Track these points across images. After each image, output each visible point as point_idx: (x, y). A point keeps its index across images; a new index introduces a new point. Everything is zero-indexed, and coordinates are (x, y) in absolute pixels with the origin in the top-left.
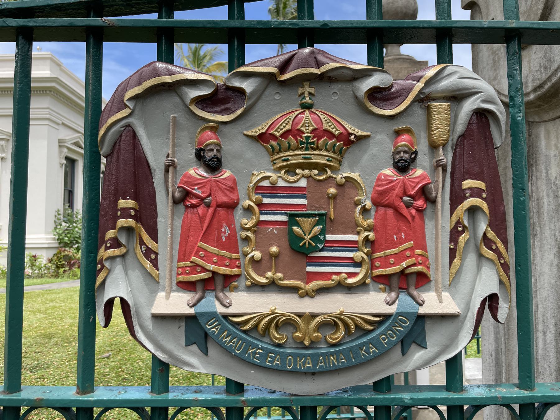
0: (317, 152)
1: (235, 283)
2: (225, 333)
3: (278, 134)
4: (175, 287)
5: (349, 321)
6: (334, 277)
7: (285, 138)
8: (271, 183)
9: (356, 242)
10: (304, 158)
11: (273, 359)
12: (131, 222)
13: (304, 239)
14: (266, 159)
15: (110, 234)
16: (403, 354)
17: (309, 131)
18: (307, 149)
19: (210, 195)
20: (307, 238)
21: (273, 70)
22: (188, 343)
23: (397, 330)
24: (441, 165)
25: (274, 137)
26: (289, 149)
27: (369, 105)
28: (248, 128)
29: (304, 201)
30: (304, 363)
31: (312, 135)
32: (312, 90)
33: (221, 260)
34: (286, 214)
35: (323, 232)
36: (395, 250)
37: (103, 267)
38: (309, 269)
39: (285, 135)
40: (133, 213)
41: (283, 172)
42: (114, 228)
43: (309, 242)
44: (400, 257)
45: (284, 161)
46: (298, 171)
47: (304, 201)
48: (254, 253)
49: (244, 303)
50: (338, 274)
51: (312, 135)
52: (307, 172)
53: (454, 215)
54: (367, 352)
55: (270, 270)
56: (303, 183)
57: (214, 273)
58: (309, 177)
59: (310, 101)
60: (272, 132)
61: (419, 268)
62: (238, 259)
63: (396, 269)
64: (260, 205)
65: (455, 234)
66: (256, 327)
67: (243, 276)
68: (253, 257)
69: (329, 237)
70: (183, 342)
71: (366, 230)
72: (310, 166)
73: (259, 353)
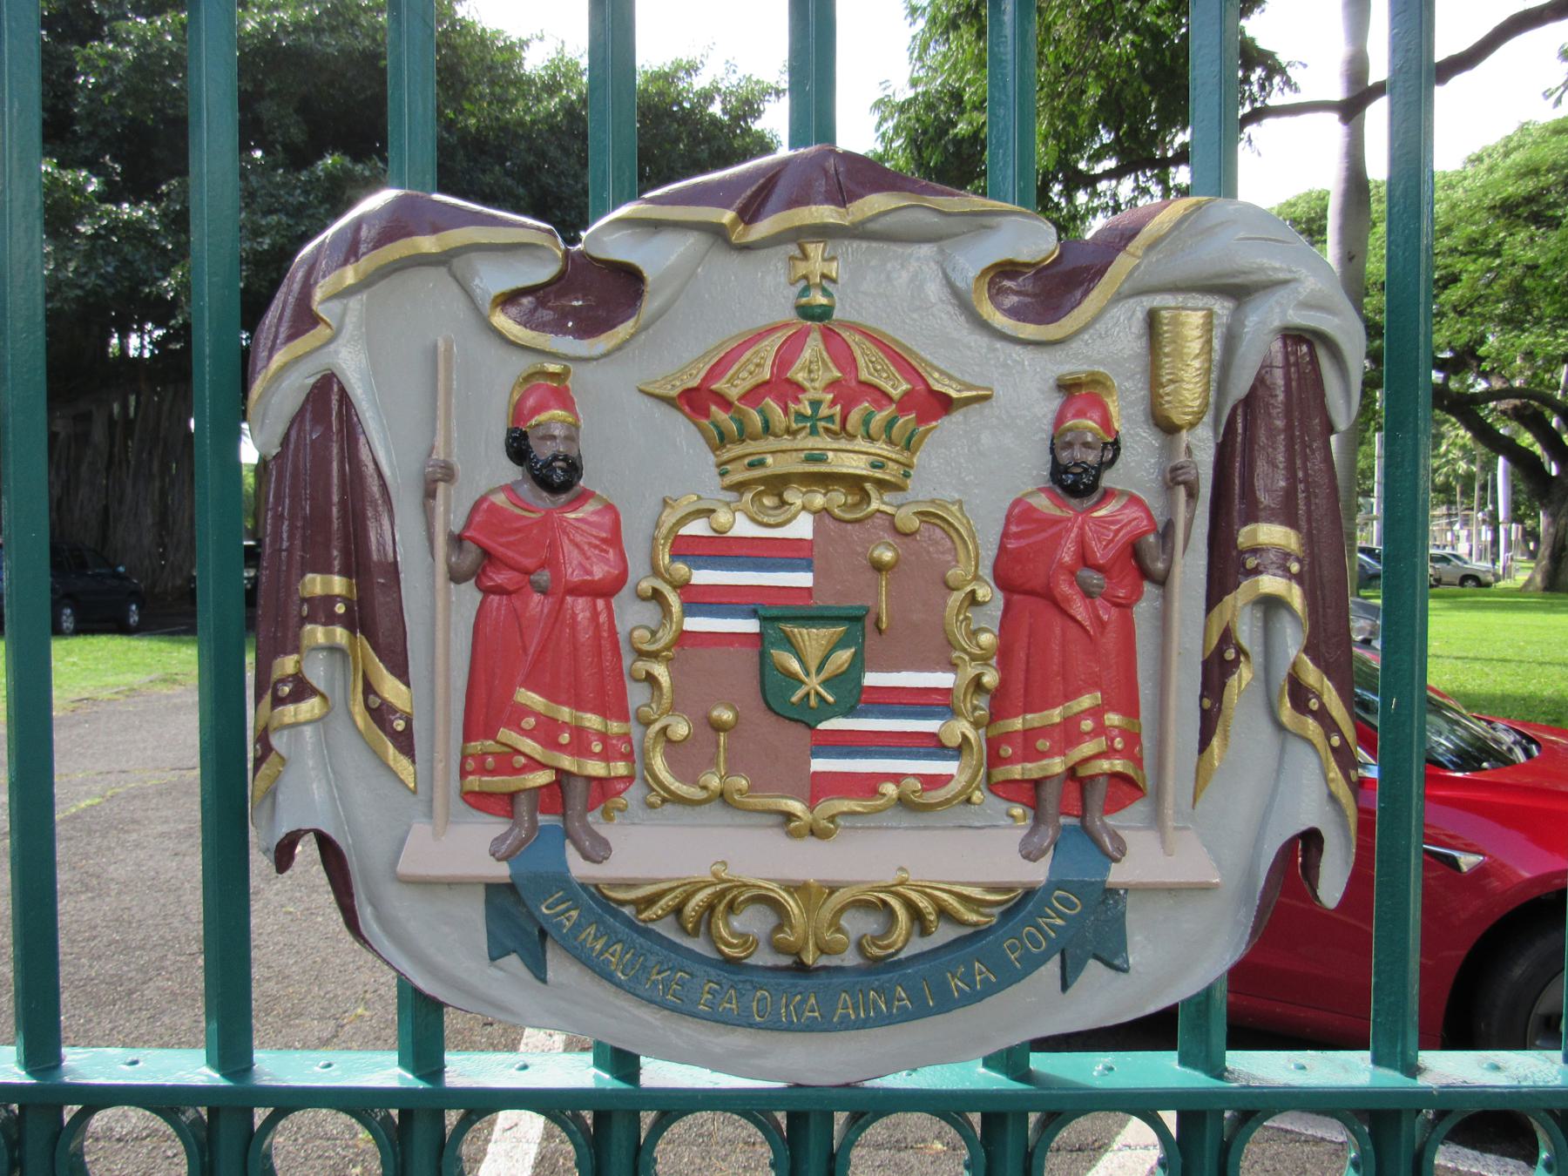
3: (733, 393)
5: (923, 903)
6: (890, 789)
12: (340, 634)
13: (802, 682)
16: (1065, 986)
24: (1185, 483)
25: (726, 404)
29: (804, 579)
34: (754, 614)
38: (819, 765)
39: (754, 395)
43: (818, 694)
44: (1069, 734)
45: (752, 465)
47: (804, 579)
49: (646, 851)
50: (896, 778)
56: (802, 528)
58: (821, 514)
59: (824, 301)
61: (1118, 765)
62: (626, 738)
65: (1217, 669)
66: (678, 911)
67: (637, 782)
69: (872, 679)
71: (973, 658)
72: (827, 480)
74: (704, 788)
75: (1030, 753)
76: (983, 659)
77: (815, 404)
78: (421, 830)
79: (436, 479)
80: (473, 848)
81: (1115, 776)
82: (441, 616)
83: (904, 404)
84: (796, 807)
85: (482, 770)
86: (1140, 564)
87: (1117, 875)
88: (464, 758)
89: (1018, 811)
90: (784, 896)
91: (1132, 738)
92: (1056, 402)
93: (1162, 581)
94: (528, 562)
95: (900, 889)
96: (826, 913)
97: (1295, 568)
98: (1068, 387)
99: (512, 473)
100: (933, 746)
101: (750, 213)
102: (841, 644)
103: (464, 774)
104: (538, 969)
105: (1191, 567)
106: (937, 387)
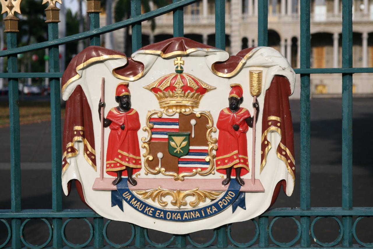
3: (162, 88)
6: (194, 170)
9: (207, 150)
11: (160, 214)
12: (80, 138)
14: (156, 101)
15: (70, 144)
17: (180, 87)
21: (159, 52)
22: (113, 204)
23: (228, 199)
25: (161, 91)
29: (177, 127)
32: (182, 62)
33: (130, 160)
37: (66, 162)
38: (180, 165)
39: (166, 89)
40: (81, 133)
42: (72, 141)
43: (180, 151)
44: (231, 159)
47: (177, 127)
50: (196, 168)
53: (263, 135)
54: (211, 210)
56: (177, 116)
57: (126, 167)
58: (180, 113)
64: (152, 128)
65: (264, 146)
66: (151, 196)
69: (191, 148)
71: (212, 143)
73: (152, 211)
82: (101, 134)
83: (197, 91)
87: (242, 188)
88: (107, 164)
95: (196, 191)
96: (182, 196)
97: (279, 124)
99: (117, 105)
100: (204, 162)
102: (184, 140)
103: (107, 168)
105: (259, 124)
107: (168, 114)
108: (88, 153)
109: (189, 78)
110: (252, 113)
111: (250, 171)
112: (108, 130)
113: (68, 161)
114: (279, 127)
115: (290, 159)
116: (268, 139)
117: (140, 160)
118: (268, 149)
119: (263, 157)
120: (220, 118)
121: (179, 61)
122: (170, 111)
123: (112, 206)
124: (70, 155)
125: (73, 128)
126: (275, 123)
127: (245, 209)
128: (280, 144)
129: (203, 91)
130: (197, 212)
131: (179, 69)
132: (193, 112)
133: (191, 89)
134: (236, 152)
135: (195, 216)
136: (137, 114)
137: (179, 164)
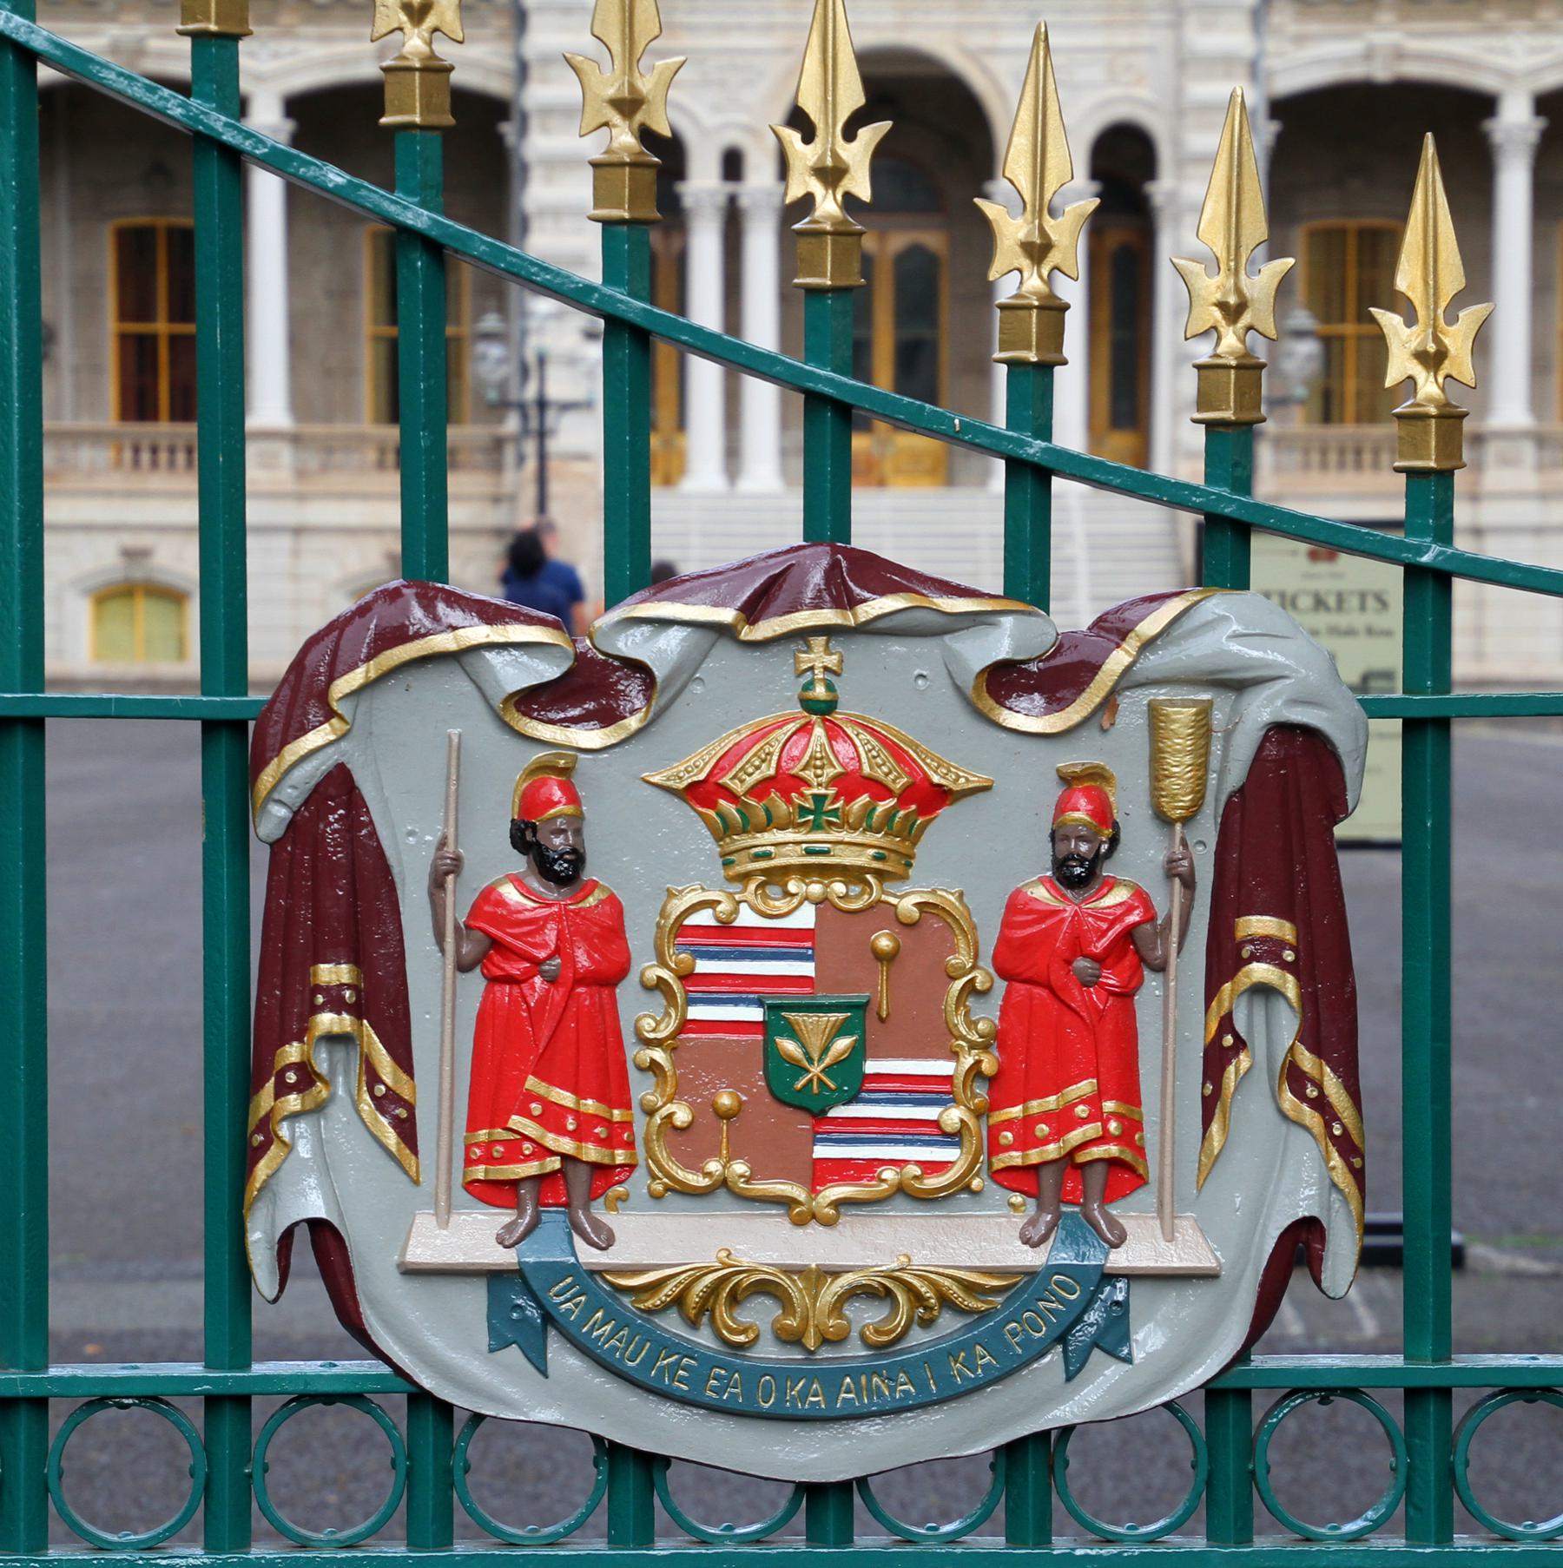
0: (845, 836)
1: (620, 1189)
2: (599, 1314)
3: (738, 788)
4: (461, 1195)
6: (889, 1174)
7: (760, 798)
8: (718, 919)
9: (948, 1079)
10: (809, 852)
12: (345, 1023)
13: (808, 1071)
15: (292, 1052)
16: (1069, 1379)
17: (823, 779)
18: (816, 827)
19: (558, 951)
20: (816, 1070)
21: (727, 615)
22: (498, 1342)
25: (733, 797)
26: (771, 823)
27: (988, 703)
28: (656, 769)
29: (807, 969)
30: (803, 1395)
31: (832, 791)
32: (831, 662)
34: (760, 1003)
35: (859, 1053)
36: (1051, 1102)
39: (760, 790)
41: (752, 887)
43: (819, 1079)
44: (1063, 1121)
46: (793, 886)
47: (807, 969)
48: (670, 1108)
49: (651, 1239)
51: (832, 791)
52: (816, 889)
55: (714, 1153)
56: (805, 918)
57: (565, 1157)
58: (822, 903)
60: (726, 780)
61: (1113, 1150)
63: (1052, 1151)
65: (1216, 1060)
66: (679, 1301)
68: (670, 1116)
69: (871, 1067)
70: (483, 1339)
71: (973, 1046)
72: (826, 872)
74: (709, 1175)
75: (1026, 1140)
76: (985, 1047)
77: (819, 799)
78: (424, 1222)
79: (445, 871)
80: (478, 1236)
81: (1113, 1163)
82: (444, 1002)
83: (904, 798)
84: (797, 1192)
85: (488, 1159)
86: (1133, 950)
88: (468, 1148)
89: (1017, 1198)
90: (785, 1281)
91: (1132, 1126)
92: (1056, 791)
93: (1161, 968)
94: (542, 954)
98: (1068, 780)
100: (937, 1133)
101: (753, 610)
102: (841, 1030)
103: (469, 1162)
104: (540, 1364)
106: (936, 779)
107: (762, 907)
108: (380, 1090)
109: (866, 736)
110: (1167, 901)
111: (1153, 1175)
112: (475, 983)
113: (284, 1131)
114: (1284, 966)
115: (1337, 1119)
116: (1240, 1025)
117: (627, 1125)
118: (1237, 1070)
119: (1209, 1106)
120: (1007, 924)
121: (819, 656)
122: (773, 890)
123: (491, 1351)
124: (293, 1102)
125: (305, 972)
126: (1270, 950)
127: (1128, 1360)
128: (1292, 1048)
129: (930, 798)
130: (902, 1377)
131: (820, 691)
132: (884, 897)
133: (879, 789)
134: (1086, 1087)
135: (892, 1390)
136: (614, 905)
137: (815, 1142)
